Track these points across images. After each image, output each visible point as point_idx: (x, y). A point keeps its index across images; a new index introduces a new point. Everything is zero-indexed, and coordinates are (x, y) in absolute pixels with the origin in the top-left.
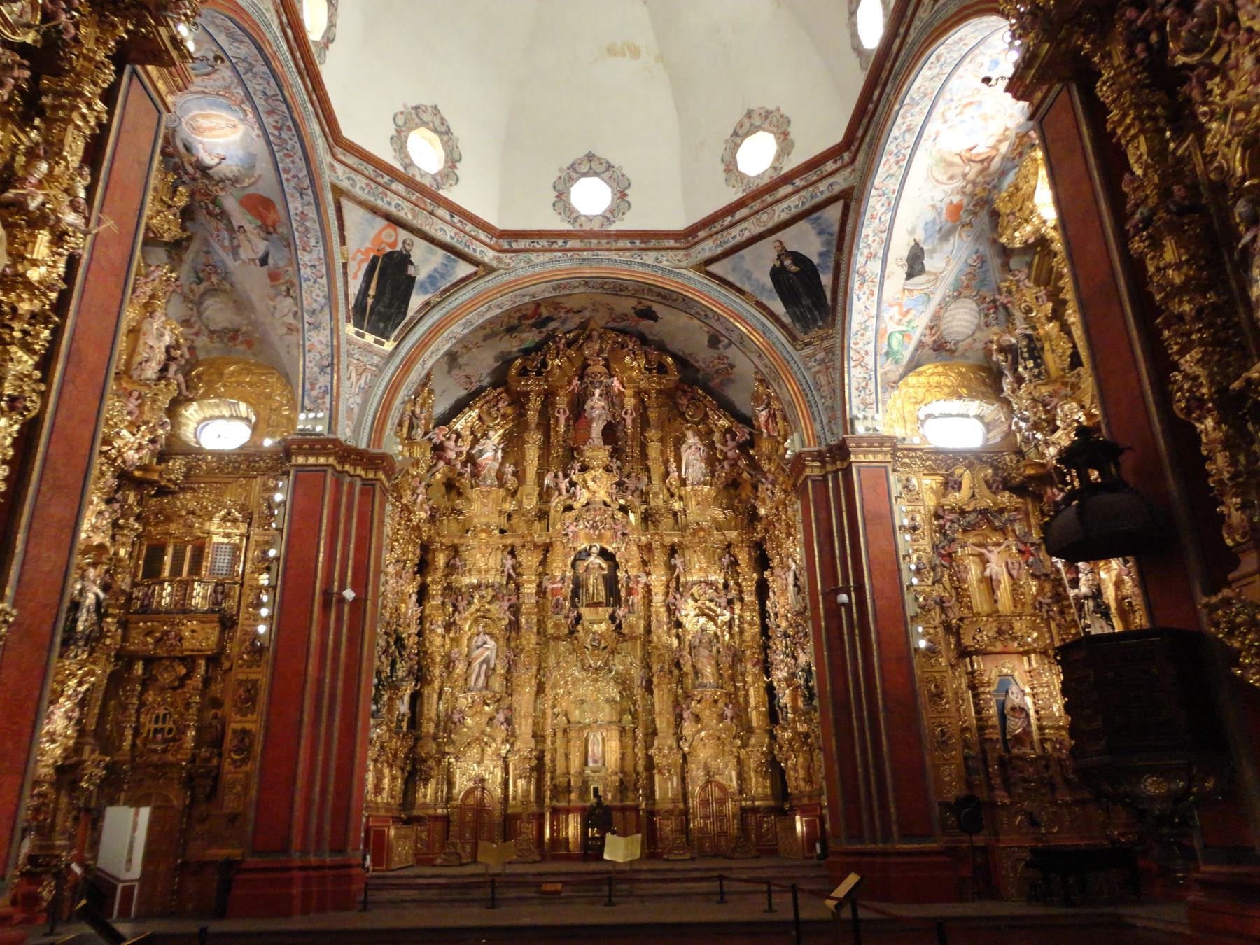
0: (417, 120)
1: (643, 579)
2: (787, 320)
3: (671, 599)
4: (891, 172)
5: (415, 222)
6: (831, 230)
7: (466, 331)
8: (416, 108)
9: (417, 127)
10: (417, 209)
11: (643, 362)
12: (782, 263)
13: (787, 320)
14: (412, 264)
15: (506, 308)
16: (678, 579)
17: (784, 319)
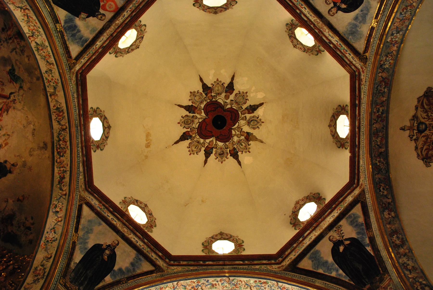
0: (139, 36)
2: (73, 266)
4: (187, 287)
5: (114, 25)
6: (136, 269)
7: (33, 45)
8: (143, 38)
9: (137, 36)
10: (116, 27)
12: (106, 249)
13: (73, 266)
14: (88, 17)
15: (45, 76)
17: (72, 263)
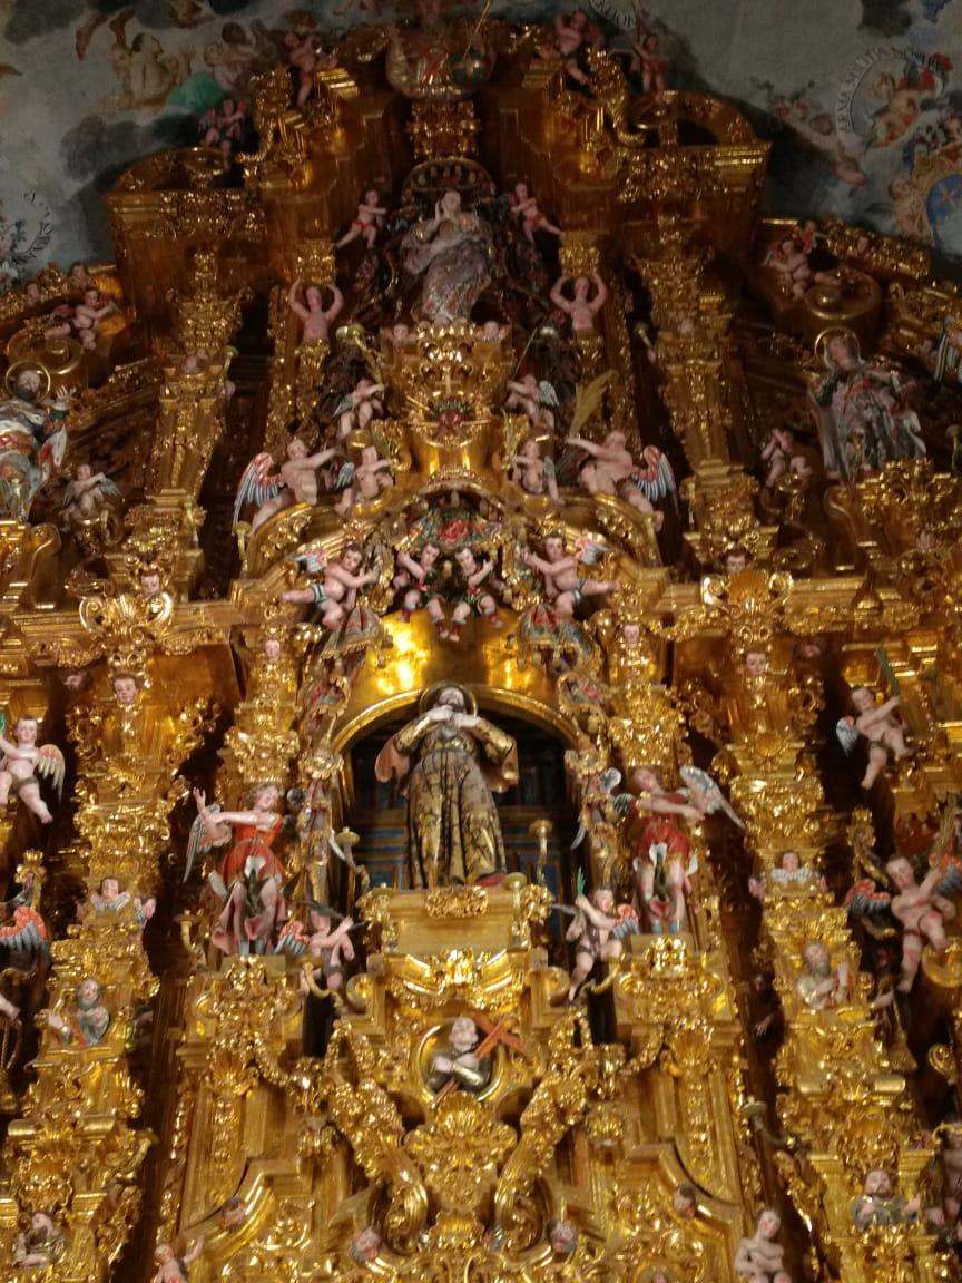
1: (702, 792)
3: (865, 894)
11: (616, 104)
16: (879, 802)
